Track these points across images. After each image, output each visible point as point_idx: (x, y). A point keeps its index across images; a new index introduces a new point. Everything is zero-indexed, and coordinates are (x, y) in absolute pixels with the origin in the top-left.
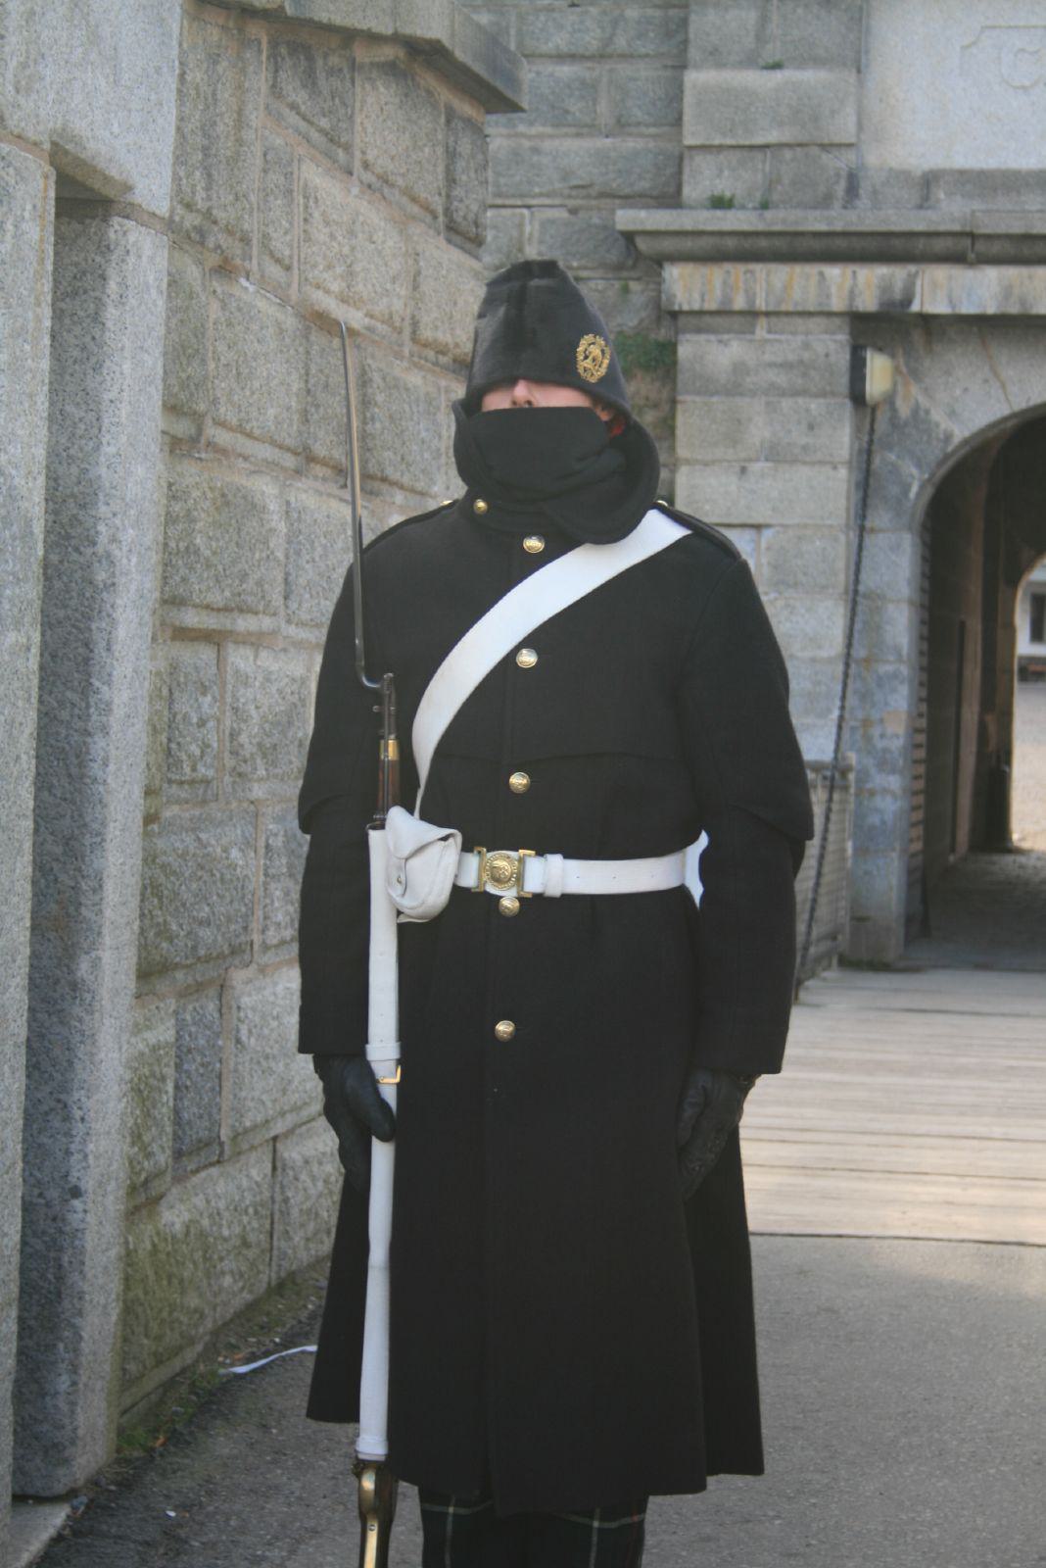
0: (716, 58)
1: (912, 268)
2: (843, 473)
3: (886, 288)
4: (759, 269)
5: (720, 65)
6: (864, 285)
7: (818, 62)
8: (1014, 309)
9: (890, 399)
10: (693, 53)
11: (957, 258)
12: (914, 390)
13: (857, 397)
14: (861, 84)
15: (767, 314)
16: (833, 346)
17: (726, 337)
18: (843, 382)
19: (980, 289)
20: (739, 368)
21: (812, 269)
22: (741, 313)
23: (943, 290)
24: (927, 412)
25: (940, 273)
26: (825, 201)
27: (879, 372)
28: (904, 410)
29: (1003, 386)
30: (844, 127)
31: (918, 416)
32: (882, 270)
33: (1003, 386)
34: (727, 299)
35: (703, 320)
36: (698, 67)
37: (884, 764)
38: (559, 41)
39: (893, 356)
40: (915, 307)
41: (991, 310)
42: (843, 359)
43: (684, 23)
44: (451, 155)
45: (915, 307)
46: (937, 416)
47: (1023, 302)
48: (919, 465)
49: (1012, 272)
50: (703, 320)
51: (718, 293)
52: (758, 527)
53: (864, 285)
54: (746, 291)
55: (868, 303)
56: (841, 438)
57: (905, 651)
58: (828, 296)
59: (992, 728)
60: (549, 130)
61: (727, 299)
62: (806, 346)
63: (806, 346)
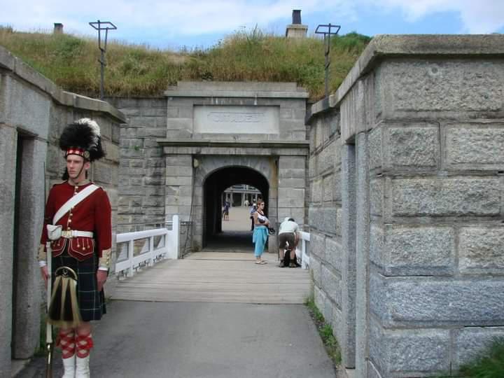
0: (172, 117)
2: (191, 178)
6: (193, 150)
9: (198, 167)
11: (207, 146)
14: (193, 121)
16: (189, 159)
18: (191, 164)
20: (175, 162)
26: (188, 137)
27: (196, 161)
28: (200, 169)
35: (170, 155)
37: (198, 222)
42: (191, 161)
44: (113, 130)
50: (170, 155)
52: (178, 186)
53: (193, 150)
55: (194, 153)
56: (190, 172)
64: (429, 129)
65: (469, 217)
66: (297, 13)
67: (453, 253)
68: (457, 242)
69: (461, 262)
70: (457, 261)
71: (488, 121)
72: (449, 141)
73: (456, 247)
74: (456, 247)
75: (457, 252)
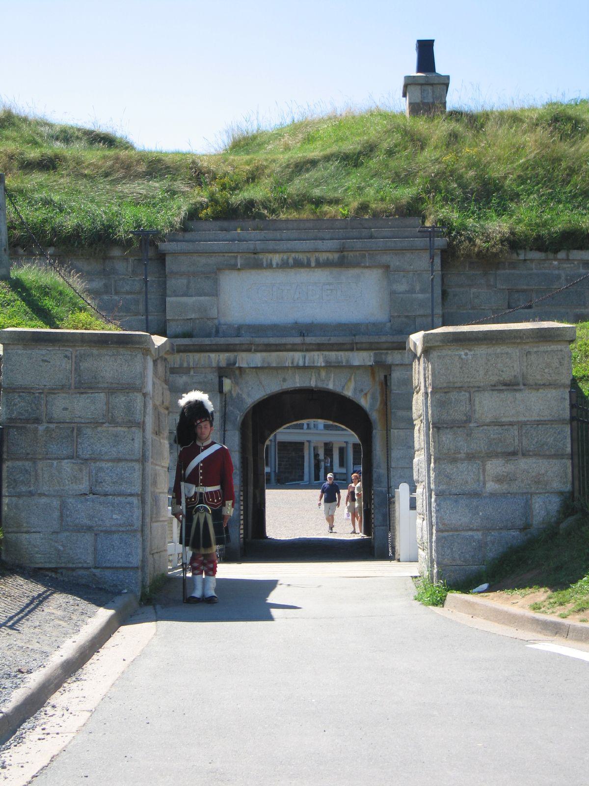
1: (235, 354)
3: (228, 359)
4: (191, 355)
5: (176, 296)
6: (222, 358)
7: (205, 295)
8: (266, 365)
9: (230, 392)
10: (168, 292)
12: (237, 388)
13: (221, 391)
15: (193, 368)
16: (213, 377)
17: (181, 375)
19: (257, 359)
21: (207, 354)
22: (186, 368)
23: (244, 359)
24: (241, 395)
25: (244, 355)
27: (227, 384)
28: (234, 395)
29: (263, 387)
30: (214, 313)
31: (239, 396)
32: (227, 355)
33: (263, 387)
34: (181, 364)
36: (170, 296)
38: (127, 288)
39: (230, 379)
40: (237, 365)
41: (259, 366)
42: (216, 380)
43: (165, 283)
45: (237, 365)
46: (244, 396)
47: (268, 363)
48: (239, 411)
49: (264, 354)
51: (179, 362)
53: (222, 358)
54: (187, 362)
55: (223, 364)
57: (238, 466)
58: (211, 363)
59: (258, 495)
60: (125, 314)
61: (181, 364)
62: (205, 377)
63: (205, 377)
64: (464, 396)
65: (492, 455)
66: (425, 50)
67: (481, 478)
68: (484, 470)
69: (488, 485)
70: (484, 484)
71: (504, 388)
72: (477, 402)
73: (484, 475)
74: (484, 475)
75: (484, 478)
